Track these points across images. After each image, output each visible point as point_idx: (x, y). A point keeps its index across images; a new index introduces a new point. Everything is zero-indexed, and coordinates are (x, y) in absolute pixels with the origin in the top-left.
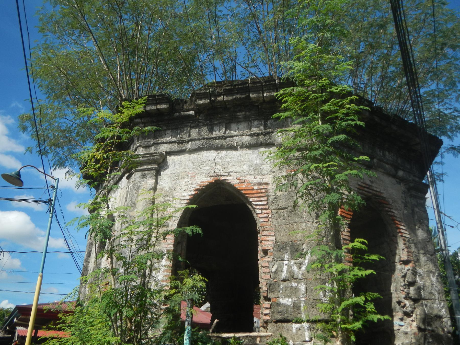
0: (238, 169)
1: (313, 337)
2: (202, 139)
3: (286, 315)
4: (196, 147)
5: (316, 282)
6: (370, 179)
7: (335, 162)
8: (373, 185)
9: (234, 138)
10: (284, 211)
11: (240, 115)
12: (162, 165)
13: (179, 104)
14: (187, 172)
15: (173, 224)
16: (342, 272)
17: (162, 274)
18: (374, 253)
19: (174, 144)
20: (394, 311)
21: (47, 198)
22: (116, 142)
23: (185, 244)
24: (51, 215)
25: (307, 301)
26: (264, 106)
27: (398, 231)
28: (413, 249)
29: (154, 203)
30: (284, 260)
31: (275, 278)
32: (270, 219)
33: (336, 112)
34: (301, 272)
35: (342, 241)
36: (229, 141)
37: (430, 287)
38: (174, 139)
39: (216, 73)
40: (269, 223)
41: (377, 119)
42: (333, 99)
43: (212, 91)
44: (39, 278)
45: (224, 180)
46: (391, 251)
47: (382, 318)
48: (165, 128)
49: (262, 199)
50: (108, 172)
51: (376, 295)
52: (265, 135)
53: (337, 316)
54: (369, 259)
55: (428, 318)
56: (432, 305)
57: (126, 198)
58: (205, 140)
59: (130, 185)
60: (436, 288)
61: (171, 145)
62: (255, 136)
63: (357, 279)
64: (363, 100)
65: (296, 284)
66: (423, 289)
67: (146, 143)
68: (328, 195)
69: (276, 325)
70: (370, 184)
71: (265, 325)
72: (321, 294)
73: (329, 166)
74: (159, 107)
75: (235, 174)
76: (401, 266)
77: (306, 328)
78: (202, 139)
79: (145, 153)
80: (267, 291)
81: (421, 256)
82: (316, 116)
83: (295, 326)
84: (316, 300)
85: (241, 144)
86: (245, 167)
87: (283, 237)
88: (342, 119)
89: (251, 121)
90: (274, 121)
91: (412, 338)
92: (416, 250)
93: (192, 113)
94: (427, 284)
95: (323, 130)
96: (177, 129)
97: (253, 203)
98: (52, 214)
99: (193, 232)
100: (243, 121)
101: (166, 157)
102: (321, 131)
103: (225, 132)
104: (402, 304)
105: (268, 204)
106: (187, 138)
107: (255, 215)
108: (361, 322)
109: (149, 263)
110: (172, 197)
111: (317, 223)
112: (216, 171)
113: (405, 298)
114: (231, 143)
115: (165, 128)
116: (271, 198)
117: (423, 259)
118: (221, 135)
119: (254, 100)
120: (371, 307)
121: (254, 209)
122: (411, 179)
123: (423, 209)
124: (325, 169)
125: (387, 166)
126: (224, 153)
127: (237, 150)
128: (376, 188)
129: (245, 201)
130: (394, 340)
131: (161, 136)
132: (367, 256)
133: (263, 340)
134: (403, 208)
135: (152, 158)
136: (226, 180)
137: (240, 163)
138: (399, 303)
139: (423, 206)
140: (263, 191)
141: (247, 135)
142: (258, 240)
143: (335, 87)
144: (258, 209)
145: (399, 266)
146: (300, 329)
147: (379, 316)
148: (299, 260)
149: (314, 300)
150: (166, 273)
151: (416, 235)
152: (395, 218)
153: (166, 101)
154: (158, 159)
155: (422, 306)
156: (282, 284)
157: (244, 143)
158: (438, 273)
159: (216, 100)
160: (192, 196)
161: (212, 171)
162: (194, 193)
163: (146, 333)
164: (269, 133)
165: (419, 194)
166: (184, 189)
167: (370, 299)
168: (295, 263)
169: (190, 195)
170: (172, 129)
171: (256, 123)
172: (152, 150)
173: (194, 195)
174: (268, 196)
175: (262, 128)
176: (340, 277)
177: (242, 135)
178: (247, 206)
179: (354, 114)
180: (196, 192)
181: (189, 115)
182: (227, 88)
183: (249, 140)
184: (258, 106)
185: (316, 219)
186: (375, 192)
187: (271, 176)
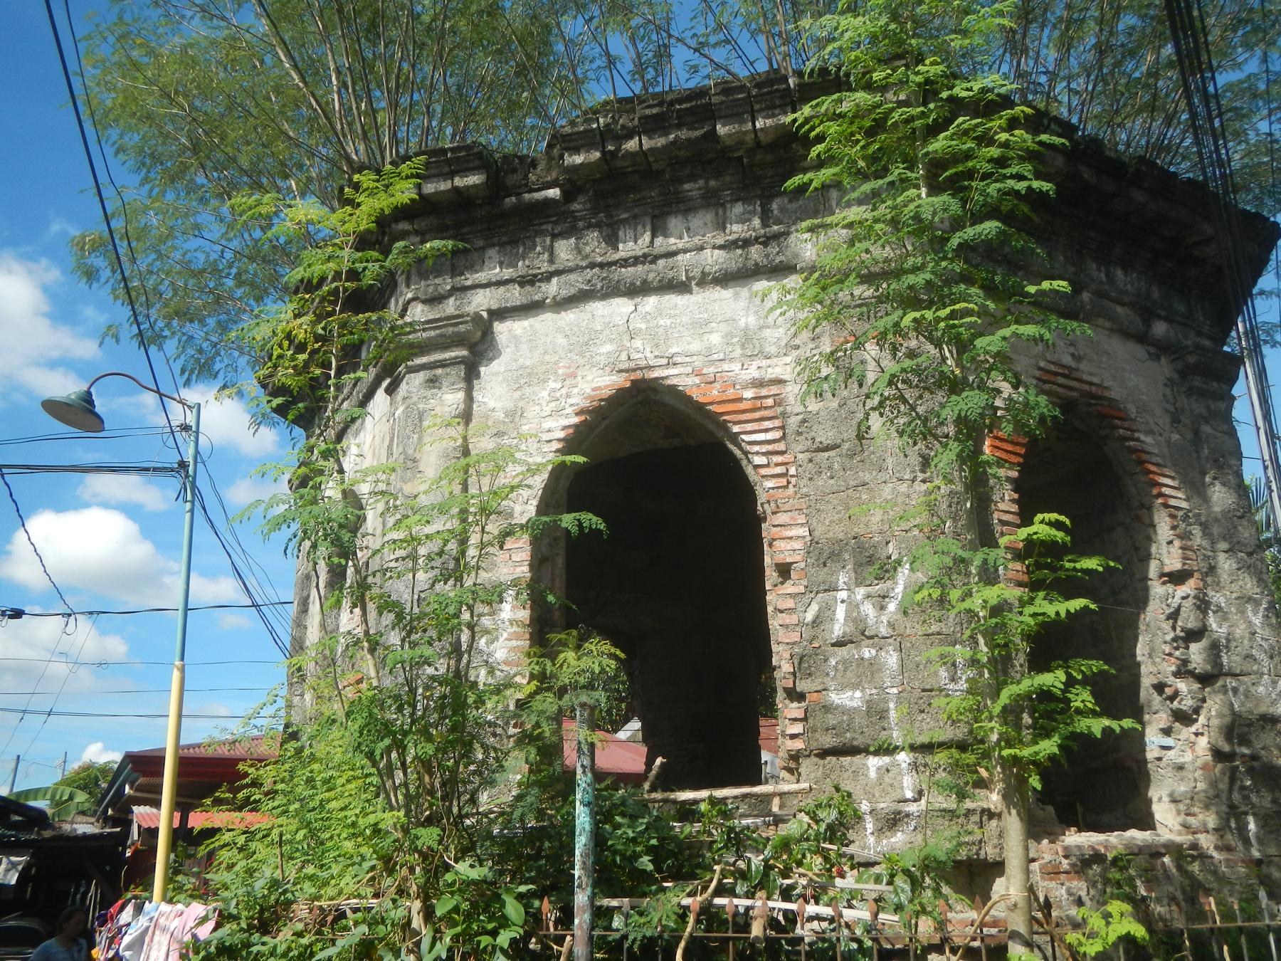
0: (695, 346)
1: (924, 786)
2: (587, 267)
3: (848, 735)
4: (573, 291)
5: (929, 642)
6: (1072, 350)
7: (969, 302)
8: (1082, 366)
9: (680, 257)
10: (832, 453)
11: (691, 188)
12: (480, 348)
13: (514, 171)
14: (553, 362)
15: (525, 507)
16: (998, 610)
17: (503, 641)
18: (1090, 554)
19: (510, 286)
20: (1146, 710)
21: (172, 459)
22: (345, 290)
23: (560, 562)
24: (188, 505)
25: (904, 694)
26: (759, 157)
27: (1155, 491)
28: (1198, 539)
29: (466, 452)
30: (836, 590)
31: (814, 638)
32: (793, 480)
33: (968, 156)
34: (884, 619)
35: (998, 528)
36: (665, 267)
37: (1246, 642)
38: (508, 273)
39: (615, 72)
40: (791, 490)
41: (1087, 174)
42: (961, 119)
43: (607, 125)
44: (176, 675)
45: (657, 378)
46: (1137, 549)
47: (1115, 725)
48: (481, 243)
49: (767, 424)
50: (332, 373)
51: (1096, 665)
52: (765, 244)
53: (991, 725)
54: (1075, 569)
55: (1240, 725)
56: (1252, 689)
57: (390, 447)
58: (596, 270)
59: (396, 409)
61: (502, 289)
62: (738, 247)
63: (1043, 625)
64: (1046, 121)
65: (873, 652)
66: (1227, 647)
67: (431, 289)
68: (954, 397)
69: (822, 762)
70: (1073, 364)
71: (793, 765)
72: (943, 673)
73: (952, 315)
74: (459, 182)
75: (688, 359)
76: (1164, 587)
77: (904, 765)
78: (587, 267)
79: (431, 317)
80: (794, 674)
81: (1222, 557)
82: (909, 174)
83: (874, 763)
84: (931, 690)
85: (698, 275)
86: (715, 339)
87: (832, 527)
88: (986, 176)
89: (723, 205)
90: (790, 201)
91: (1195, 780)
92: (1205, 543)
93: (554, 193)
95: (935, 213)
96: (514, 242)
97: (743, 437)
98: (193, 502)
99: (580, 525)
100: (702, 207)
101: (491, 326)
102: (926, 215)
103: (652, 242)
104: (1168, 691)
105: (784, 437)
106: (545, 267)
107: (749, 470)
108: (1056, 739)
109: (466, 616)
110: (515, 434)
111: (924, 481)
112: (635, 356)
113: (1177, 674)
114: (671, 274)
115: (481, 243)
116: (793, 422)
117: (1226, 564)
118: (640, 253)
119: (728, 143)
120: (1082, 698)
121: (746, 453)
122: (1189, 342)
123: (1225, 427)
124: (942, 325)
125: (1119, 309)
126: (651, 302)
127: (690, 292)
128: (1091, 374)
129: (720, 434)
131: (472, 268)
132: (1069, 561)
133: (788, 803)
134: (1167, 427)
135: (451, 329)
136: (663, 378)
137: (701, 327)
138: (1160, 688)
139: (1227, 418)
140: (770, 402)
141: (714, 247)
142: (762, 539)
143: (965, 85)
144: (757, 453)
145: (1157, 589)
146: (888, 771)
147: (1106, 722)
148: (880, 587)
149: (924, 690)
150: (514, 643)
151: (1206, 500)
152: (1145, 457)
153: (477, 163)
154: (468, 331)
155: (1225, 692)
156: (834, 654)
157: (707, 269)
158: (1269, 602)
159: (618, 149)
160: (571, 431)
161: (624, 357)
162: (576, 420)
163: (473, 801)
164: (776, 237)
165: (1215, 384)
166: (547, 410)
167: (1080, 677)
168: (868, 596)
169: (564, 428)
170: (502, 245)
171: (738, 209)
172: (450, 307)
173: (576, 426)
174: (784, 415)
175: (757, 222)
176: (994, 620)
177: (702, 248)
178: (727, 449)
179: (1022, 159)
180: (583, 418)
181: (548, 202)
182: (648, 112)
183: (721, 260)
184: (740, 159)
185: (923, 471)
186: (1086, 387)
187: (788, 359)
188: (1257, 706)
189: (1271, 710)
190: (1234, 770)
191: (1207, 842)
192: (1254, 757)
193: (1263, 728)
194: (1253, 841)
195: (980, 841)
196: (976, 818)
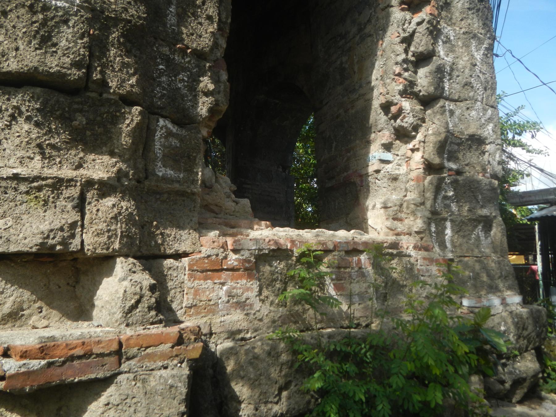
37: (467, 71)
55: (451, 143)
56: (466, 114)
60: (481, 75)
66: (450, 74)
76: (403, 13)
91: (406, 190)
94: (461, 63)
113: (404, 93)
130: (367, 198)
138: (386, 107)
155: (443, 113)
188: (467, 128)
189: (479, 132)
190: (441, 180)
191: (408, 244)
192: (459, 172)
193: (470, 147)
194: (448, 245)
195: (73, 226)
196: (75, 192)
